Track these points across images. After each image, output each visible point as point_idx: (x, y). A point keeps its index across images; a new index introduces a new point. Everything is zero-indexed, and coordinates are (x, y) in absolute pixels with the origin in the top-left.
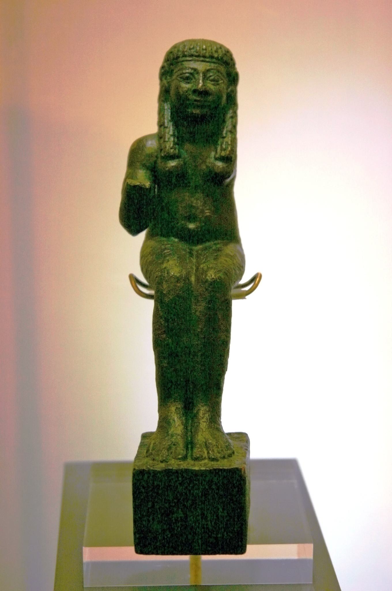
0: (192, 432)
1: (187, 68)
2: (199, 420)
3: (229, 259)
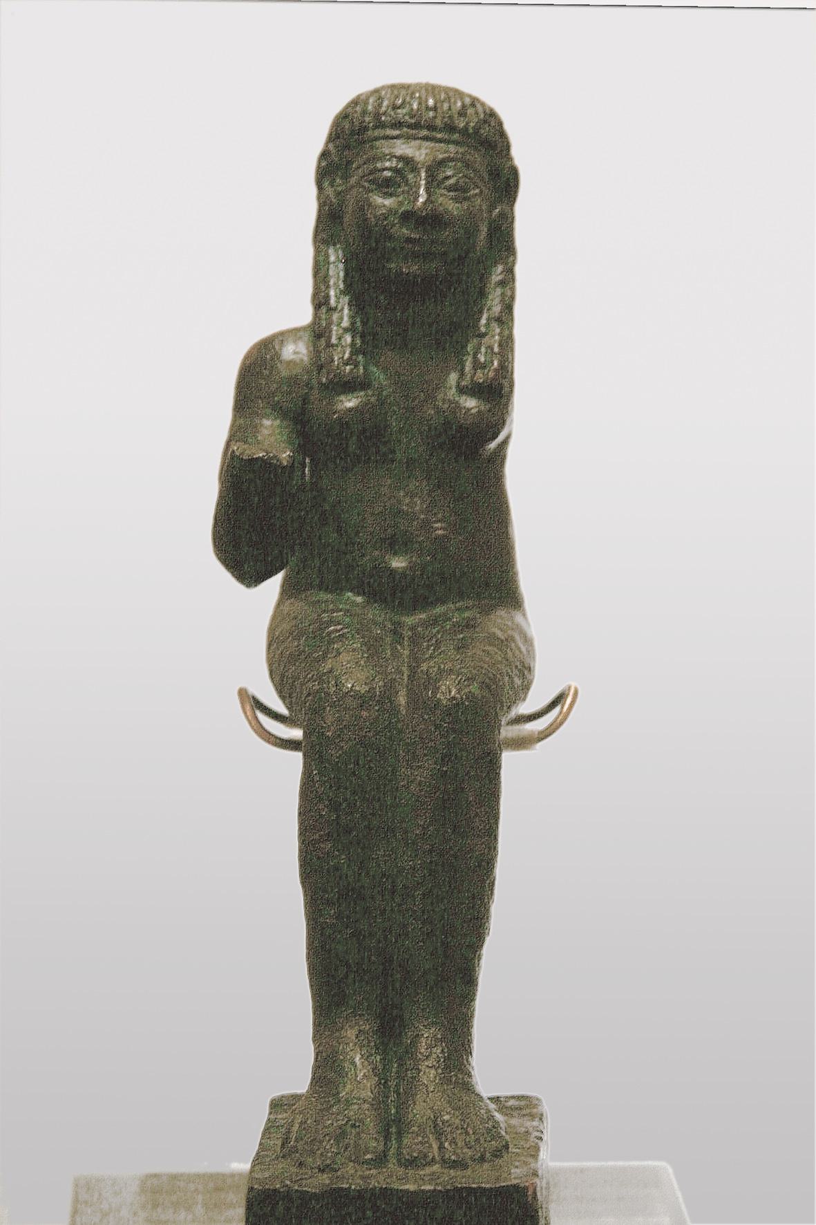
0: (399, 1094)
1: (388, 157)
2: (417, 1061)
3: (495, 649)
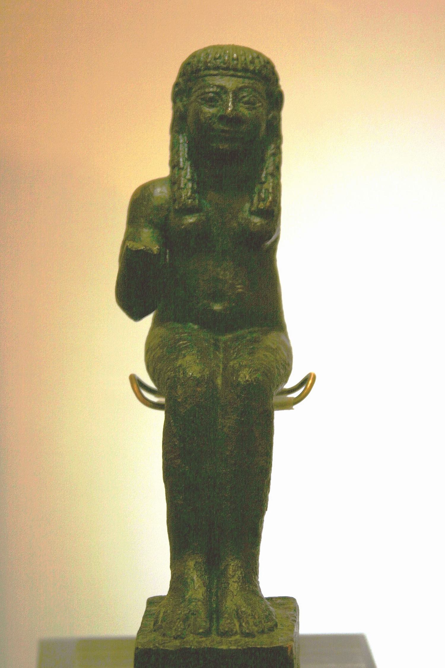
0: (217, 597)
1: (212, 86)
